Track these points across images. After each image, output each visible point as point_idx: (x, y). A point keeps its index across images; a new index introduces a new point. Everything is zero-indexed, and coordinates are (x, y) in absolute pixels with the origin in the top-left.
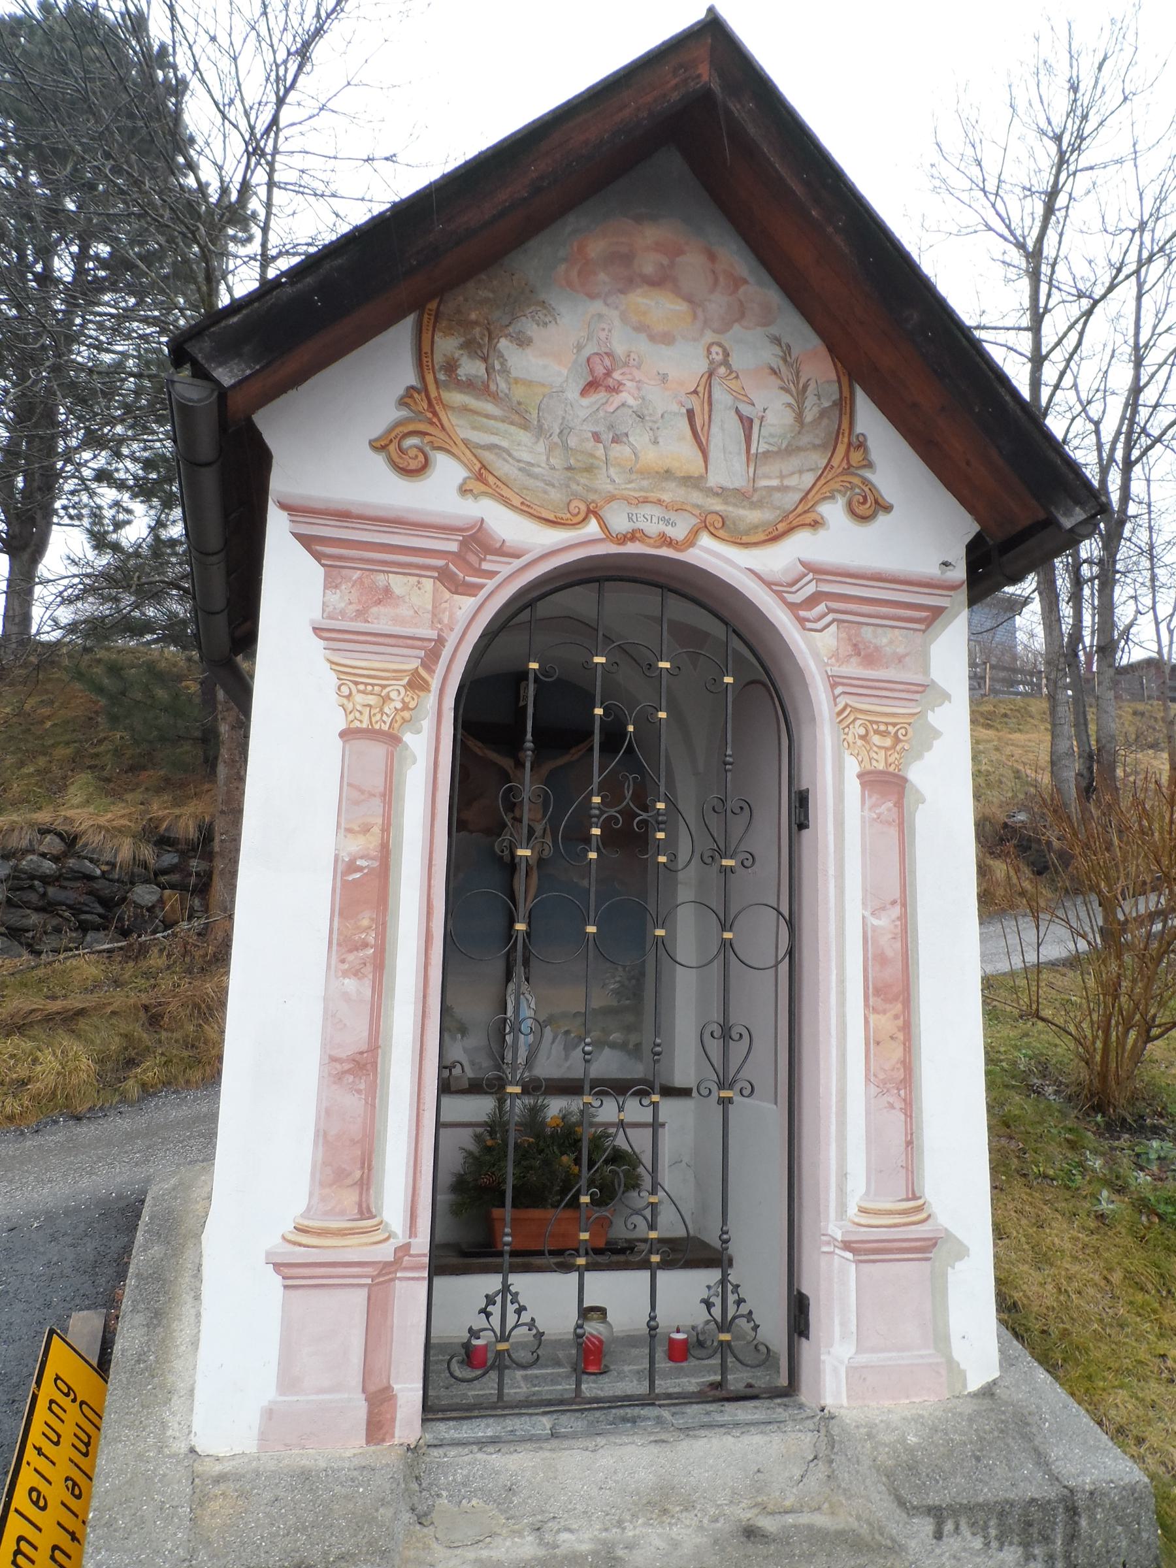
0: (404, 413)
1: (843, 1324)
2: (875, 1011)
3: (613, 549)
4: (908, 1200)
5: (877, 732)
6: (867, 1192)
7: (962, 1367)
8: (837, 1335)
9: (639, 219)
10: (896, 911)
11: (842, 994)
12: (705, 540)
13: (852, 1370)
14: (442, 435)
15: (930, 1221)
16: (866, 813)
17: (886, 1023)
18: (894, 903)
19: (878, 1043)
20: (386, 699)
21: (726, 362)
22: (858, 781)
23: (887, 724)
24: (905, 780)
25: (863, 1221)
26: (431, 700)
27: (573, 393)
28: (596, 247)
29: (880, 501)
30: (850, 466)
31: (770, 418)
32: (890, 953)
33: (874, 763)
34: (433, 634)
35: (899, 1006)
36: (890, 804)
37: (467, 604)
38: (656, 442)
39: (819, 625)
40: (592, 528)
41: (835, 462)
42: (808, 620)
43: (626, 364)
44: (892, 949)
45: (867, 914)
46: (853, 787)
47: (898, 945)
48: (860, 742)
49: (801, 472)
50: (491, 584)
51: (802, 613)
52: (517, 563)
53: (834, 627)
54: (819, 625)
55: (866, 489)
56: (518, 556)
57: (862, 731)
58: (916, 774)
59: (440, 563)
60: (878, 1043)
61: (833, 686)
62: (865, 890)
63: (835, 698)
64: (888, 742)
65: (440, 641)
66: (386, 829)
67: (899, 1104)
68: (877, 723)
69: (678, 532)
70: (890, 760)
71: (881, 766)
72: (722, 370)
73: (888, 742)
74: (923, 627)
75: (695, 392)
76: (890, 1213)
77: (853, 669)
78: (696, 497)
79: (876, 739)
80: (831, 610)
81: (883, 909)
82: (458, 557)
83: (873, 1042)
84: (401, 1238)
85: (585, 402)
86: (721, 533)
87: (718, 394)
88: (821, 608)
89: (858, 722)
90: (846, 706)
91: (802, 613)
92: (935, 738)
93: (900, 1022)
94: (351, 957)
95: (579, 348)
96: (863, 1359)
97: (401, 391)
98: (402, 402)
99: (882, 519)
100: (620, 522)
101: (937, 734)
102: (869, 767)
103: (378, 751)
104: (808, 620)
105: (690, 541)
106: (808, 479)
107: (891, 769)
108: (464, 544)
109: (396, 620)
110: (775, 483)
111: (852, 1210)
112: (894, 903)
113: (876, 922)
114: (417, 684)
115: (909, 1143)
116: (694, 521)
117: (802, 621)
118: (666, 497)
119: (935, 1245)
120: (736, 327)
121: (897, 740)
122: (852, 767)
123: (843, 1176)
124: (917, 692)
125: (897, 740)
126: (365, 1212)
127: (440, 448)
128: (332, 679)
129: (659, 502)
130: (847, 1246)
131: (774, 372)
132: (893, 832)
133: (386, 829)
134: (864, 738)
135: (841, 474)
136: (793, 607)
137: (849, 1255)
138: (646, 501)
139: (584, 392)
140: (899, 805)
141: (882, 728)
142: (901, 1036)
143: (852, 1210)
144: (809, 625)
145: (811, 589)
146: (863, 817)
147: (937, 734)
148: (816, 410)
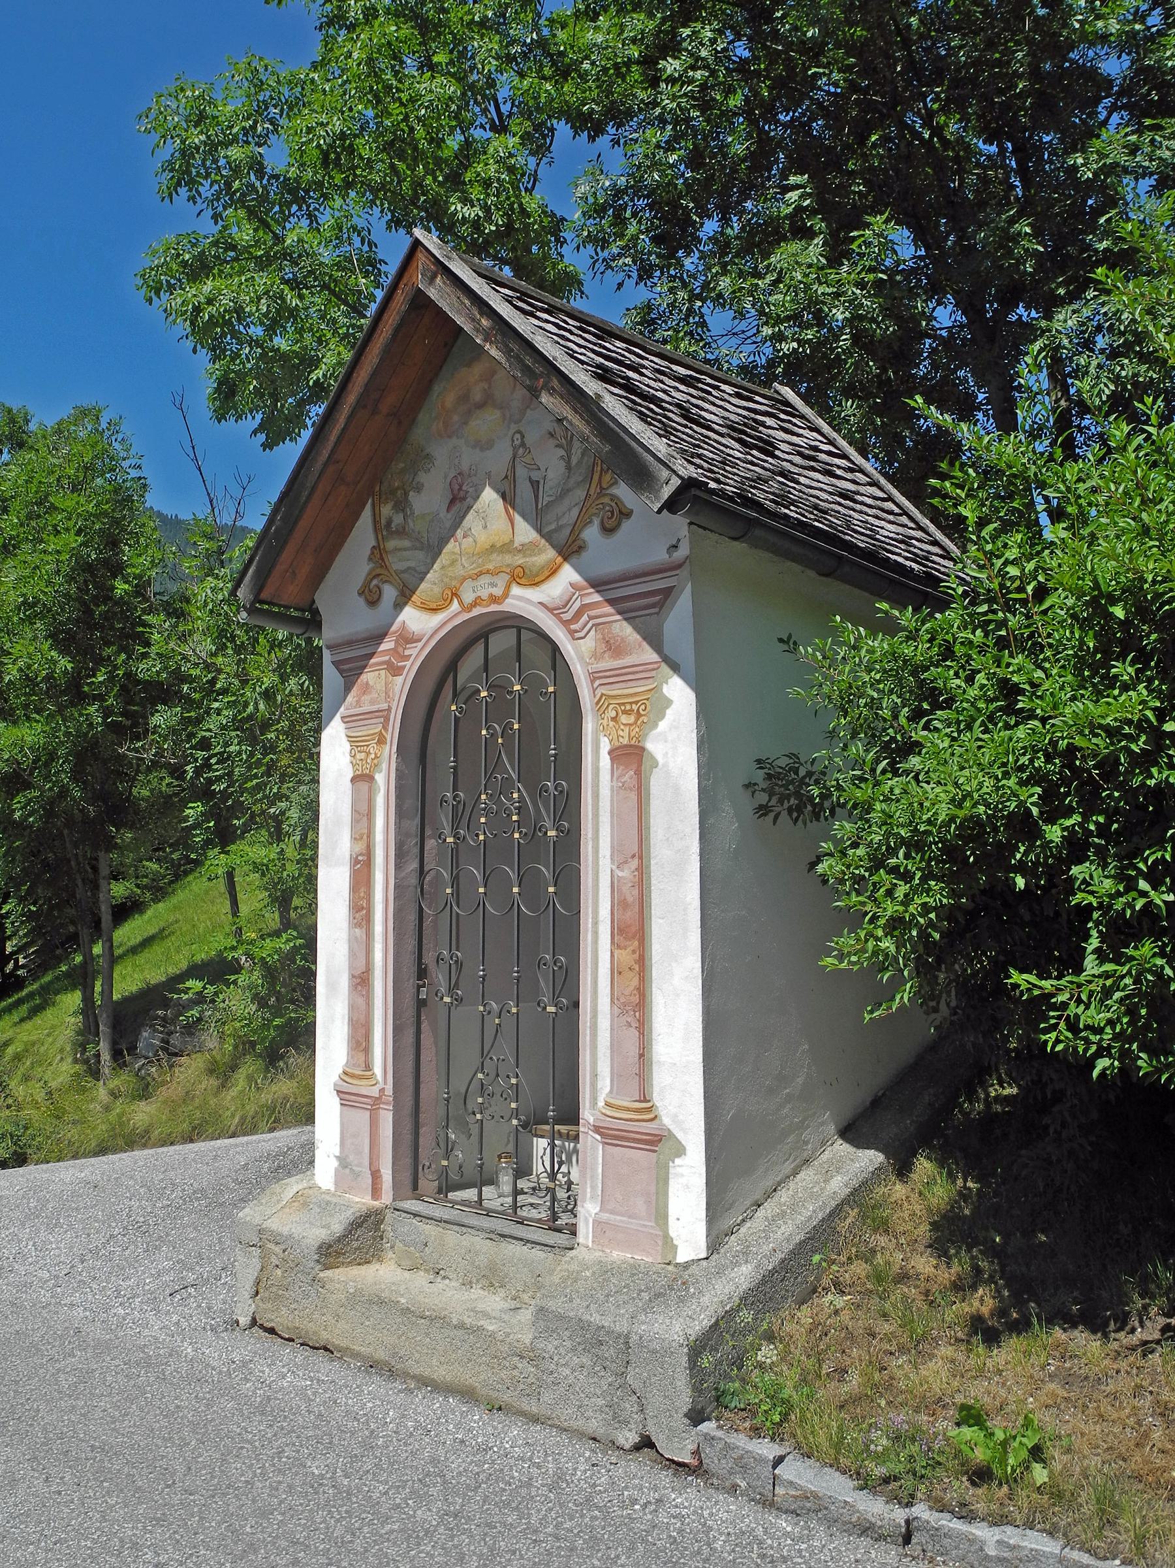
0: (372, 565)
1: (593, 1188)
2: (619, 947)
3: (466, 616)
4: (640, 1101)
5: (624, 712)
6: (611, 1091)
7: (675, 1242)
8: (589, 1195)
9: (469, 365)
10: (635, 863)
11: (596, 933)
12: (516, 590)
13: (597, 1222)
14: (386, 573)
15: (656, 1121)
16: (615, 783)
17: (626, 957)
18: (633, 856)
19: (620, 973)
20: (368, 753)
21: (523, 444)
22: (608, 757)
23: (631, 703)
24: (643, 749)
25: (608, 1113)
26: (388, 747)
27: (443, 514)
28: (450, 399)
29: (624, 510)
30: (602, 488)
31: (551, 475)
32: (630, 899)
33: (621, 740)
34: (385, 706)
35: (636, 943)
36: (632, 773)
37: (399, 680)
38: (485, 527)
39: (582, 634)
40: (455, 606)
41: (592, 492)
42: (577, 631)
43: (469, 476)
44: (631, 895)
45: (614, 867)
46: (605, 761)
47: (636, 892)
48: (612, 724)
49: (569, 510)
50: (408, 664)
51: (573, 627)
52: (420, 645)
53: (593, 632)
54: (582, 634)
55: (613, 504)
56: (419, 640)
57: (613, 714)
58: (650, 746)
59: (387, 658)
60: (620, 973)
61: (592, 682)
62: (612, 847)
63: (594, 691)
64: (632, 719)
65: (389, 709)
66: (369, 837)
67: (635, 1024)
68: (624, 704)
69: (498, 591)
70: (633, 734)
71: (625, 741)
72: (521, 451)
73: (632, 719)
74: (656, 610)
75: (506, 477)
76: (628, 1110)
77: (608, 663)
78: (508, 559)
79: (624, 719)
80: (591, 618)
81: (626, 862)
82: (395, 650)
83: (616, 972)
84: (381, 1085)
85: (449, 516)
86: (523, 581)
87: (521, 472)
88: (585, 617)
89: (611, 707)
90: (602, 695)
91: (573, 627)
92: (667, 707)
93: (636, 956)
94: (357, 915)
95: (445, 477)
96: (605, 1216)
97: (368, 552)
98: (370, 559)
99: (626, 525)
100: (468, 597)
101: (669, 703)
102: (617, 744)
103: (364, 786)
104: (577, 631)
105: (506, 594)
106: (575, 512)
107: (632, 742)
108: (397, 642)
109: (372, 702)
110: (553, 527)
111: (601, 1104)
112: (633, 856)
113: (620, 874)
114: (381, 741)
115: (641, 1056)
116: (507, 577)
117: (572, 633)
118: (490, 566)
119: (660, 1140)
120: (528, 411)
121: (639, 715)
122: (605, 746)
123: (595, 1076)
124: (653, 670)
125: (639, 715)
126: (368, 1067)
127: (386, 581)
128: (347, 746)
129: (488, 572)
130: (597, 1129)
131: (551, 435)
132: (633, 796)
133: (369, 837)
134: (614, 719)
135: (597, 498)
136: (566, 623)
137: (598, 1137)
138: (481, 574)
139: (448, 510)
140: (638, 773)
141: (628, 707)
142: (637, 967)
143: (601, 1104)
144: (577, 635)
145: (577, 605)
146: (612, 787)
147: (669, 703)
148: (579, 451)
